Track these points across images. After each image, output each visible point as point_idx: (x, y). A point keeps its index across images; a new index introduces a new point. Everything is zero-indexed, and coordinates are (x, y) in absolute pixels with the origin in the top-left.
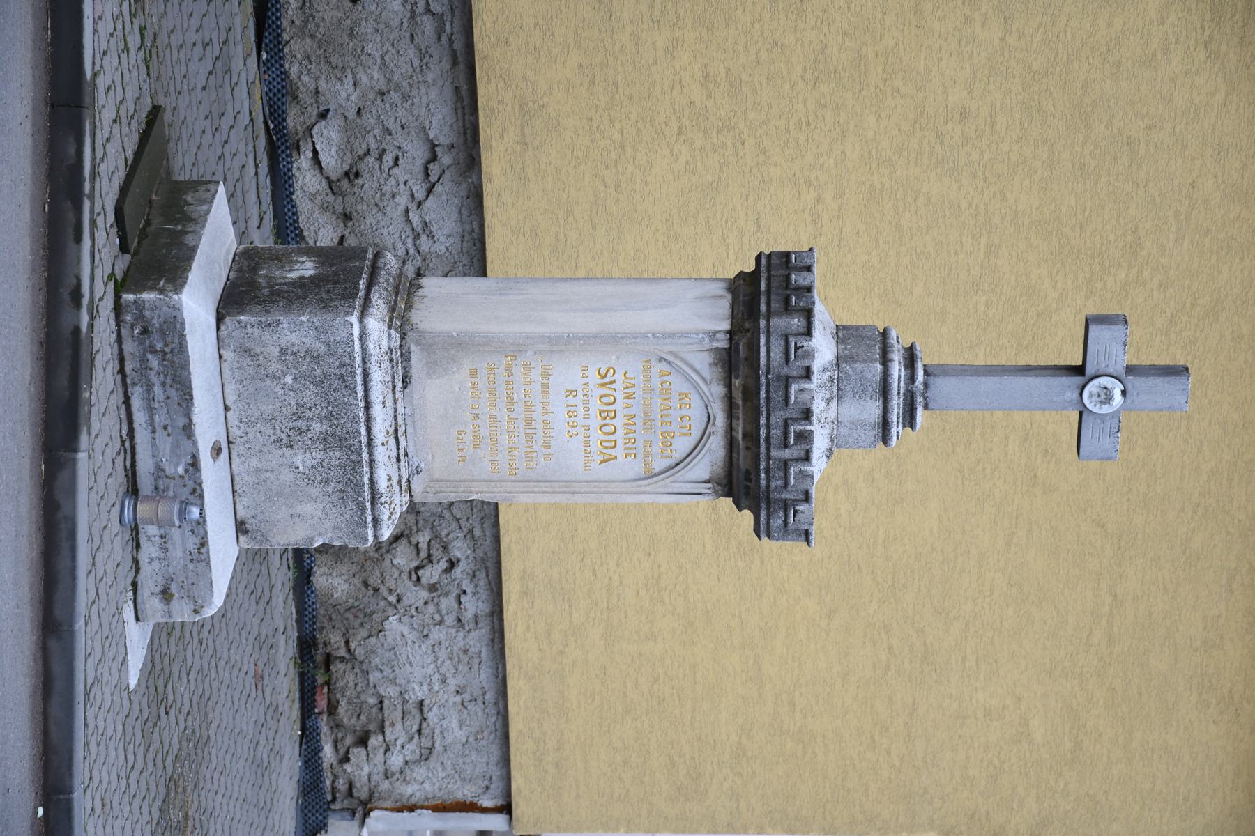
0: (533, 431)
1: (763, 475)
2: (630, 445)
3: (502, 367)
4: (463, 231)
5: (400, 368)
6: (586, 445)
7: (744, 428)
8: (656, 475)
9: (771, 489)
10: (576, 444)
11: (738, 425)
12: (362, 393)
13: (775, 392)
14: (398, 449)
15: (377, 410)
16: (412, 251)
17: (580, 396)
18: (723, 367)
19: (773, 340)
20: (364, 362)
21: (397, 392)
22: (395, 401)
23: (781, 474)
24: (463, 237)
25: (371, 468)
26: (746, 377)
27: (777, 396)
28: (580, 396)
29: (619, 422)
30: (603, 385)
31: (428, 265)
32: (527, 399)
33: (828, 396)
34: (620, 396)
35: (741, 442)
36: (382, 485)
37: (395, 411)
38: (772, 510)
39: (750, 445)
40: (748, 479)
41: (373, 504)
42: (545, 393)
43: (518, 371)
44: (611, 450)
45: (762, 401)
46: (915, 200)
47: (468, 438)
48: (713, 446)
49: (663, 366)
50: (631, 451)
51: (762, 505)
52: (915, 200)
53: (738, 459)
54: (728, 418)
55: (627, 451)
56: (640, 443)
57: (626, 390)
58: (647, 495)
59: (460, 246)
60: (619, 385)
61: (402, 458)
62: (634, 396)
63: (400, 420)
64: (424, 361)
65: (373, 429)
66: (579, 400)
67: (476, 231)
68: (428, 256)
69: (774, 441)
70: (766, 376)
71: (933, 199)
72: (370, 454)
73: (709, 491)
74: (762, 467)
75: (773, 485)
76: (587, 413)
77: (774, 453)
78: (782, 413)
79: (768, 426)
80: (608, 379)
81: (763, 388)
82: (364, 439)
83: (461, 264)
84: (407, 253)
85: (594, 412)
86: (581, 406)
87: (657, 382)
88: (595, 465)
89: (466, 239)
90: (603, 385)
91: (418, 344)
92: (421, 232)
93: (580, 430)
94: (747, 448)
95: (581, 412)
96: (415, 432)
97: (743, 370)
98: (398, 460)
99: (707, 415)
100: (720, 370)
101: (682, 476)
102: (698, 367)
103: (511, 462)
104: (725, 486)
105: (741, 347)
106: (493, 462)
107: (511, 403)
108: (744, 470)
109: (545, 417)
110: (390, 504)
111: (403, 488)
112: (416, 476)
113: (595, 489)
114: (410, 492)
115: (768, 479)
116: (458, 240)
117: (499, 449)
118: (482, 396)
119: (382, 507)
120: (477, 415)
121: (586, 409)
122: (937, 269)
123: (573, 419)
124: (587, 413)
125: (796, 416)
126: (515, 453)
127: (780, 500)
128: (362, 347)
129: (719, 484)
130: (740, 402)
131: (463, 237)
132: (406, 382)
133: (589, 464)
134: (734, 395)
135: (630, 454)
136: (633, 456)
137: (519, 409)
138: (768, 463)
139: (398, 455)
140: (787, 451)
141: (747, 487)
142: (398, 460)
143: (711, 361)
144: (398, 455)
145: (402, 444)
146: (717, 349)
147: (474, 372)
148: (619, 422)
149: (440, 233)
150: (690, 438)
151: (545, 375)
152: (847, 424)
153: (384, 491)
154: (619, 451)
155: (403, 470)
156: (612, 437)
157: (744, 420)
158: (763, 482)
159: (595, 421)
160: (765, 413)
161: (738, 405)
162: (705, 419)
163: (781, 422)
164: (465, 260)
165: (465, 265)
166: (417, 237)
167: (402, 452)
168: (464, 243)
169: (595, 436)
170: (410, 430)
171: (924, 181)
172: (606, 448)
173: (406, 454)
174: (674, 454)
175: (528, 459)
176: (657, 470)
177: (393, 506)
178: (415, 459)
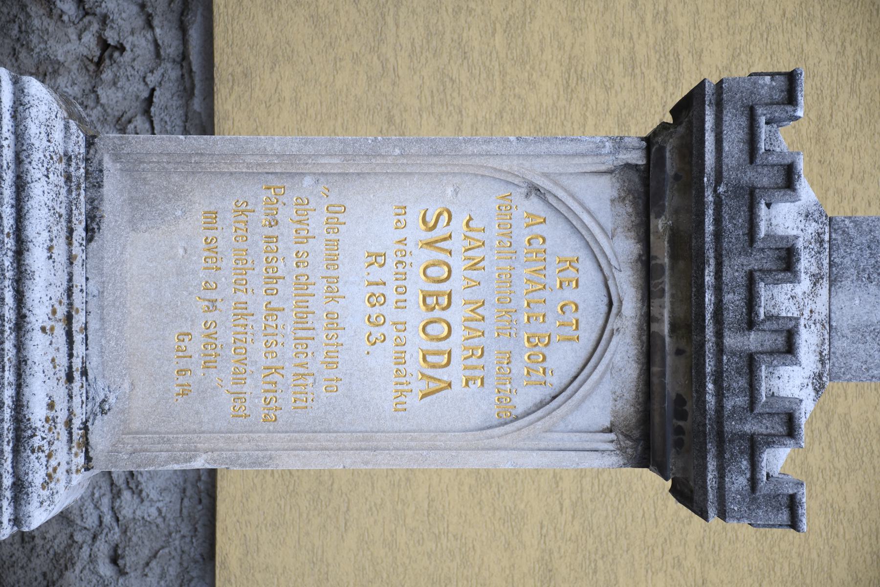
0: (309, 334)
1: (710, 386)
2: (474, 361)
3: (261, 209)
4: (185, 481)
5: (82, 197)
6: (400, 360)
7: (672, 312)
8: (517, 418)
9: (726, 414)
10: (385, 353)
11: (662, 307)
12: (12, 222)
13: (732, 218)
14: (71, 356)
15: (36, 258)
16: (108, 518)
17: (391, 262)
18: (634, 203)
19: (727, 117)
20: (18, 160)
21: (75, 243)
22: (71, 260)
23: (743, 382)
24: (184, 491)
25: (19, 375)
26: (676, 212)
27: (735, 228)
28: (391, 262)
29: (457, 315)
30: (429, 244)
31: (130, 539)
32: (301, 270)
33: (814, 269)
34: (458, 263)
35: (667, 339)
36: (37, 412)
37: (70, 280)
38: (727, 456)
39: (683, 344)
40: (681, 415)
41: (16, 451)
42: (332, 261)
43: (287, 214)
44: (440, 371)
45: (708, 238)
46: (827, 426)
47: (195, 347)
48: (618, 358)
49: (535, 205)
50: (478, 373)
51: (709, 446)
52: (827, 426)
53: (663, 374)
54: (642, 300)
55: (468, 373)
56: (491, 358)
57: (470, 253)
58: (503, 453)
59: (178, 507)
60: (457, 244)
61: (77, 375)
62: (481, 265)
63: (78, 299)
64: (126, 196)
65: (27, 294)
66: (387, 274)
67: (203, 478)
68: (131, 525)
69: (729, 316)
70: (715, 191)
71: (854, 425)
72: (19, 346)
73: (611, 447)
74: (708, 369)
75: (729, 405)
76: (402, 297)
77: (731, 341)
78: (742, 260)
79: (718, 290)
80: (440, 232)
81: (710, 212)
82: (9, 314)
83: (178, 536)
84: (101, 522)
85: (414, 297)
86: (392, 285)
87: (522, 236)
88: (413, 401)
89: (188, 493)
90: (429, 244)
91: (116, 157)
92: (123, 486)
93: (388, 329)
94: (679, 352)
95: (392, 297)
96: (103, 329)
97: (671, 199)
98: (70, 378)
99: (606, 300)
100: (630, 210)
101: (563, 418)
102: (593, 206)
103: (270, 395)
104: (636, 441)
105: (668, 154)
106: (238, 397)
107: (272, 279)
108: (674, 395)
109: (332, 306)
110: (49, 456)
111: (76, 437)
112: (99, 416)
113: (412, 444)
114: (87, 452)
115: (720, 394)
116: (176, 496)
117: (248, 368)
118: (223, 265)
119: (33, 457)
120: (213, 302)
121: (402, 290)
122: (866, 539)
123: (377, 310)
124: (402, 297)
125: (767, 266)
126: (277, 377)
127: (742, 436)
128: (15, 133)
129: (627, 436)
130: (666, 260)
131: (184, 491)
132: (91, 233)
133: (403, 399)
134: (653, 253)
135: (475, 380)
136: (479, 382)
137: (286, 288)
138: (719, 362)
139: (70, 367)
140: (752, 335)
141: (679, 431)
142: (70, 378)
143: (615, 194)
144: (70, 367)
145: (79, 349)
146: (628, 166)
147: (212, 216)
148: (457, 315)
149: (151, 485)
150: (575, 345)
151: (333, 225)
152: (846, 332)
153: (39, 424)
154: (455, 373)
155: (77, 400)
156: (444, 346)
157: (672, 296)
158: (710, 399)
159: (415, 315)
160: (712, 261)
161: (662, 266)
162: (604, 308)
163: (741, 277)
164: (185, 529)
165: (183, 537)
166: (116, 494)
167: (77, 363)
168: (186, 500)
169: (417, 342)
170: (93, 325)
171: (839, 396)
172: (434, 366)
173: (84, 373)
174: (549, 378)
175: (297, 389)
176: (520, 410)
177: (53, 463)
178: (100, 384)
